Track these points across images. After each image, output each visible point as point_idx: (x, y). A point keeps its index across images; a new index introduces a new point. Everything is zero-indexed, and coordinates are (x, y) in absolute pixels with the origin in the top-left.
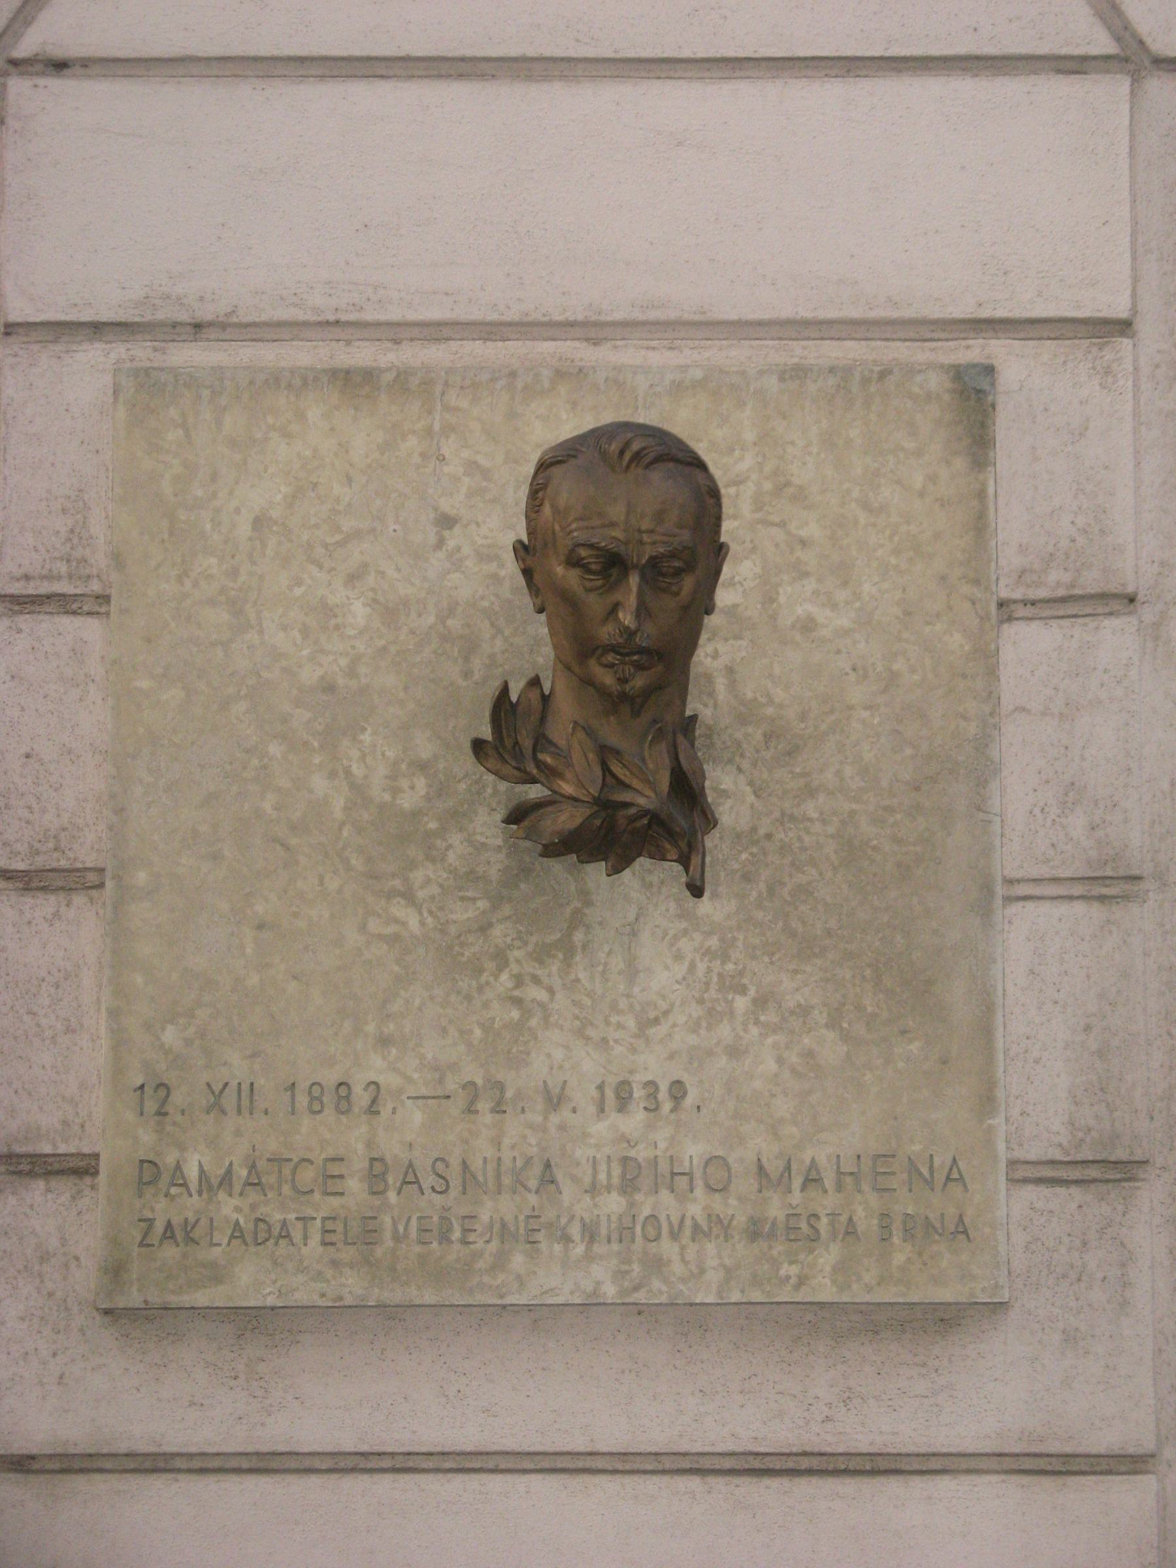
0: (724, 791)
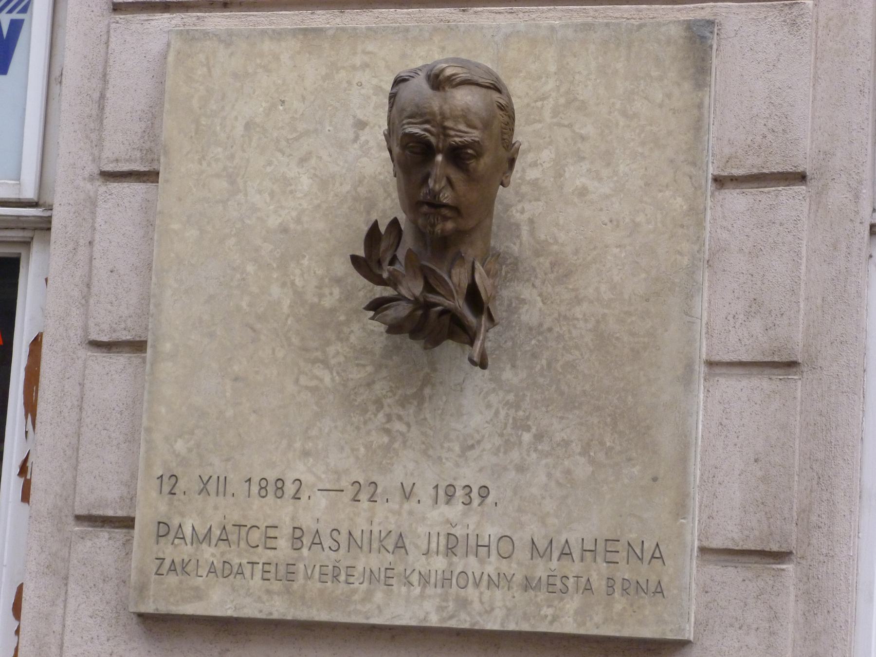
0: (524, 300)
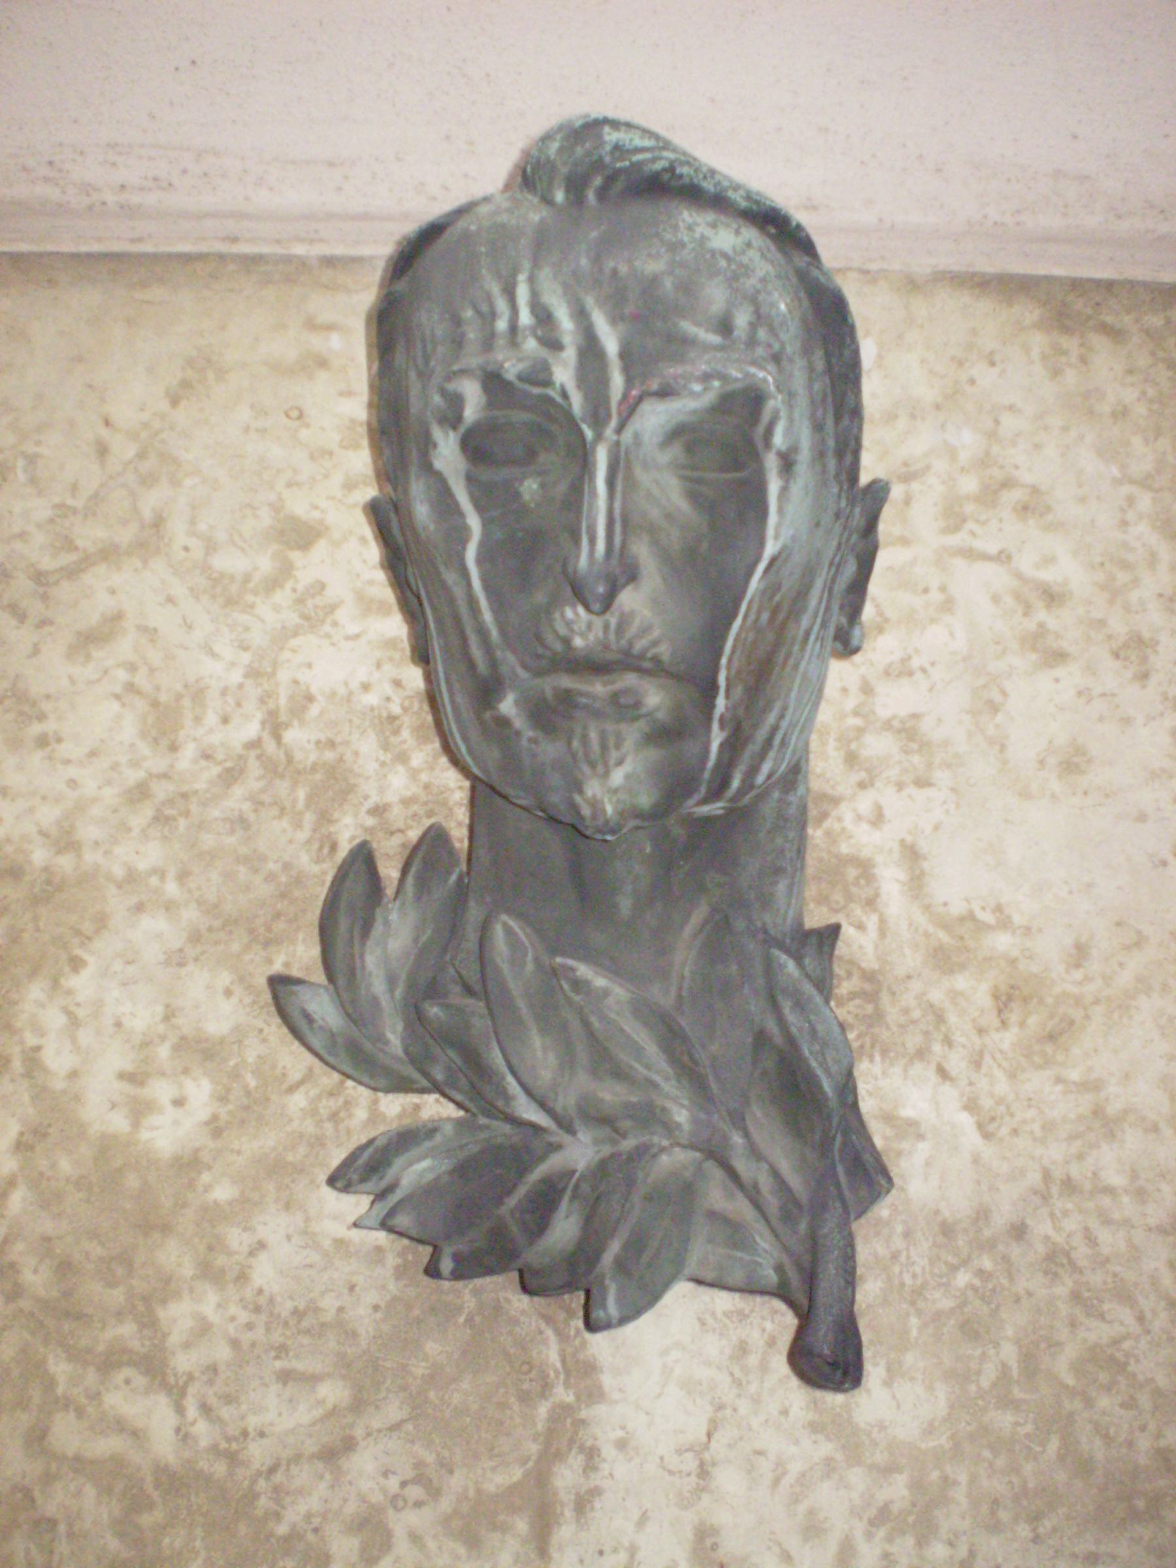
0: (912, 1123)
